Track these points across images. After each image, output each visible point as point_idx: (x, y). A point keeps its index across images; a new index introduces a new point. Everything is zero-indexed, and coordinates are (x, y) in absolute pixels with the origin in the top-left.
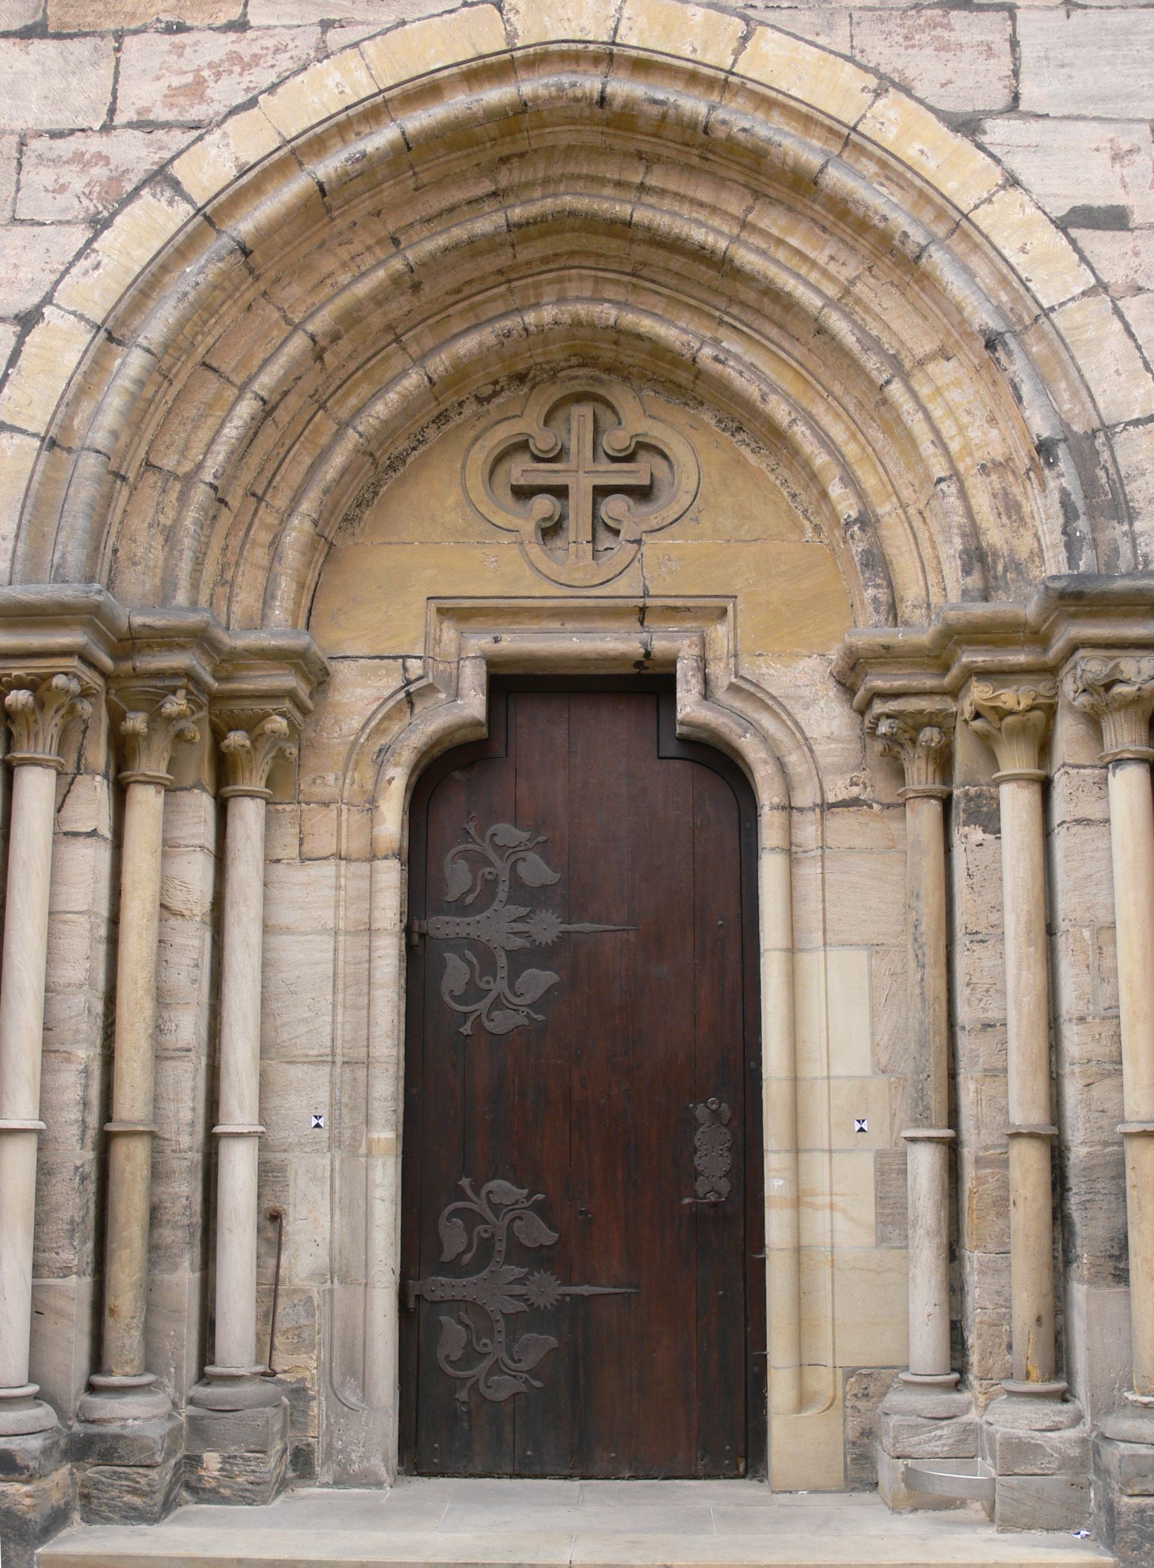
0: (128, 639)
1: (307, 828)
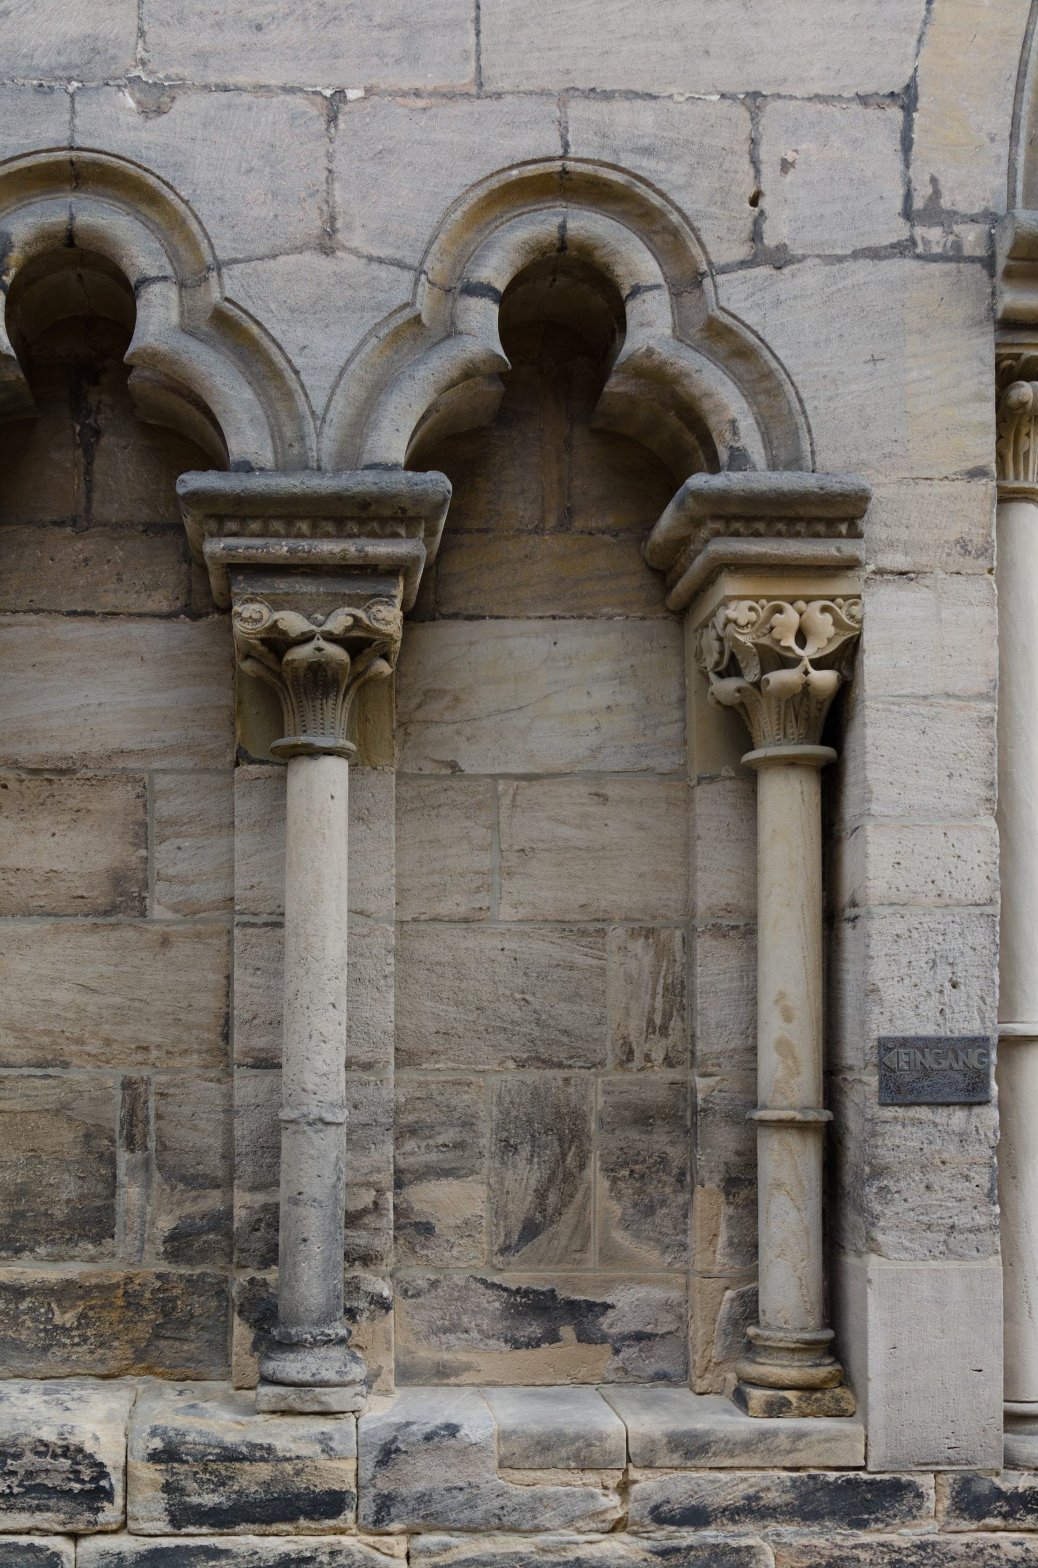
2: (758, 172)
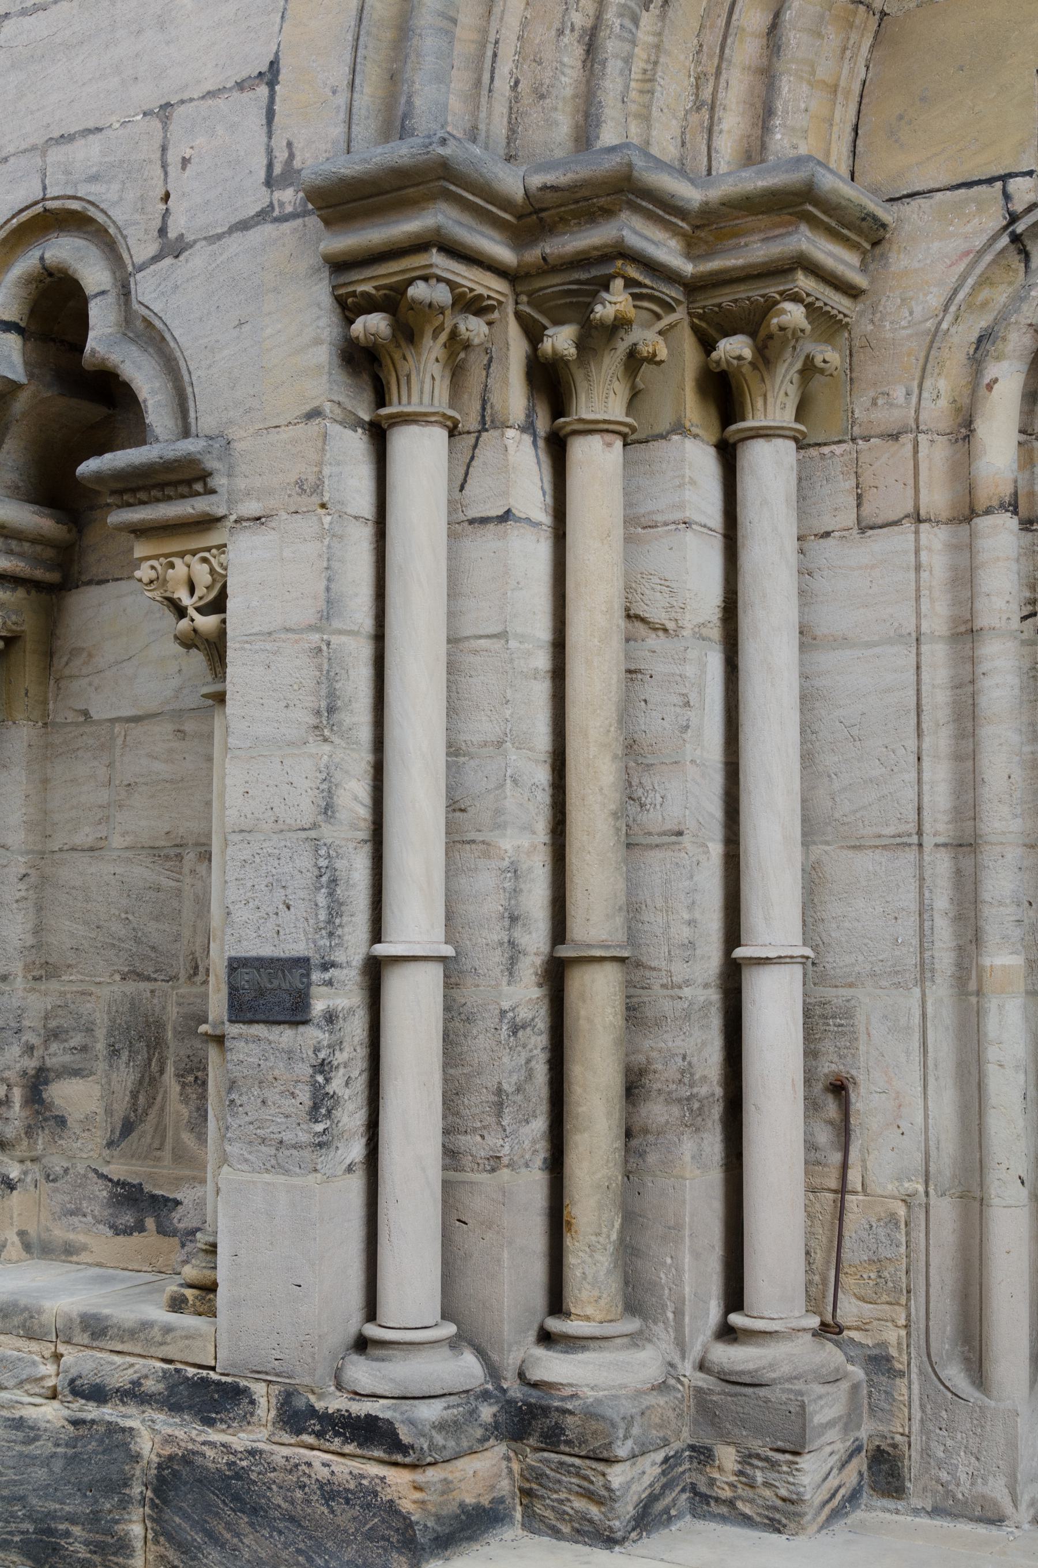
0: (530, 214)
1: (867, 479)
2: (166, 173)
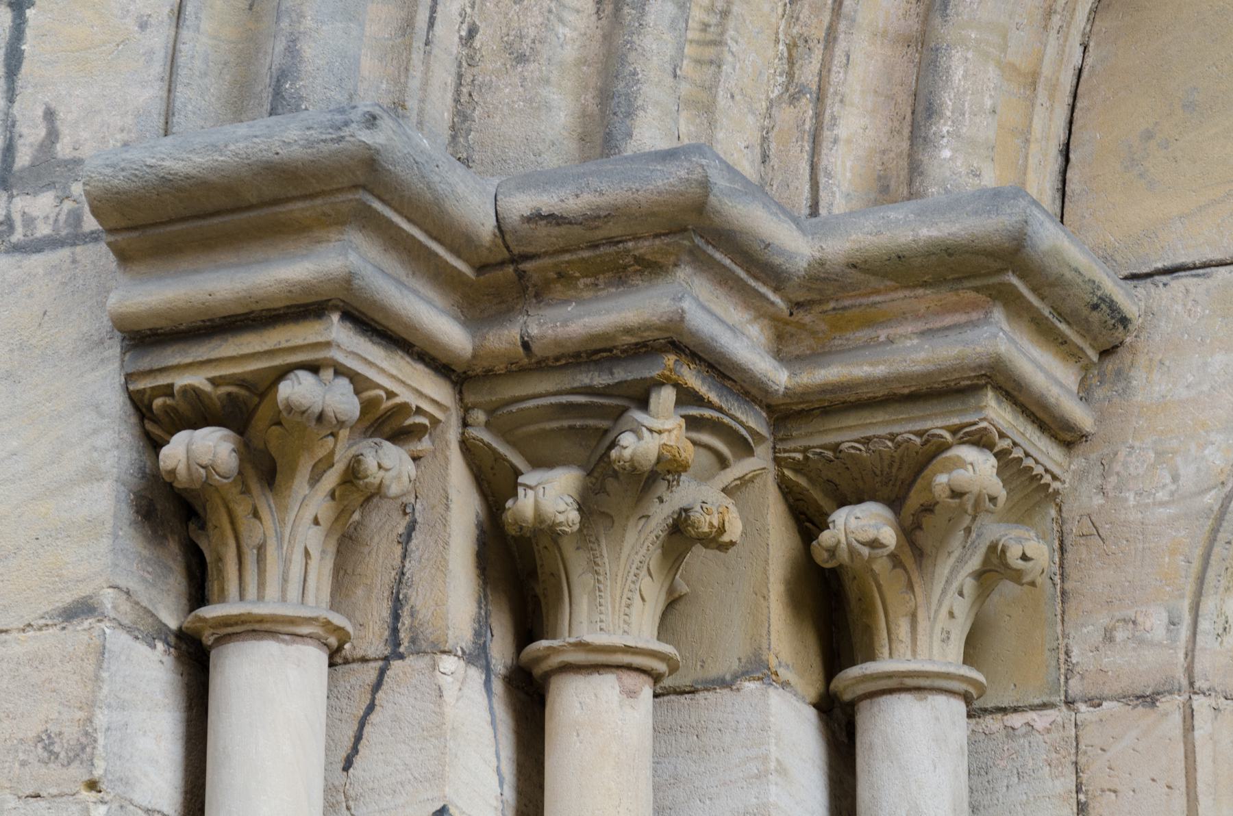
0: (502, 264)
1: (1096, 777)
